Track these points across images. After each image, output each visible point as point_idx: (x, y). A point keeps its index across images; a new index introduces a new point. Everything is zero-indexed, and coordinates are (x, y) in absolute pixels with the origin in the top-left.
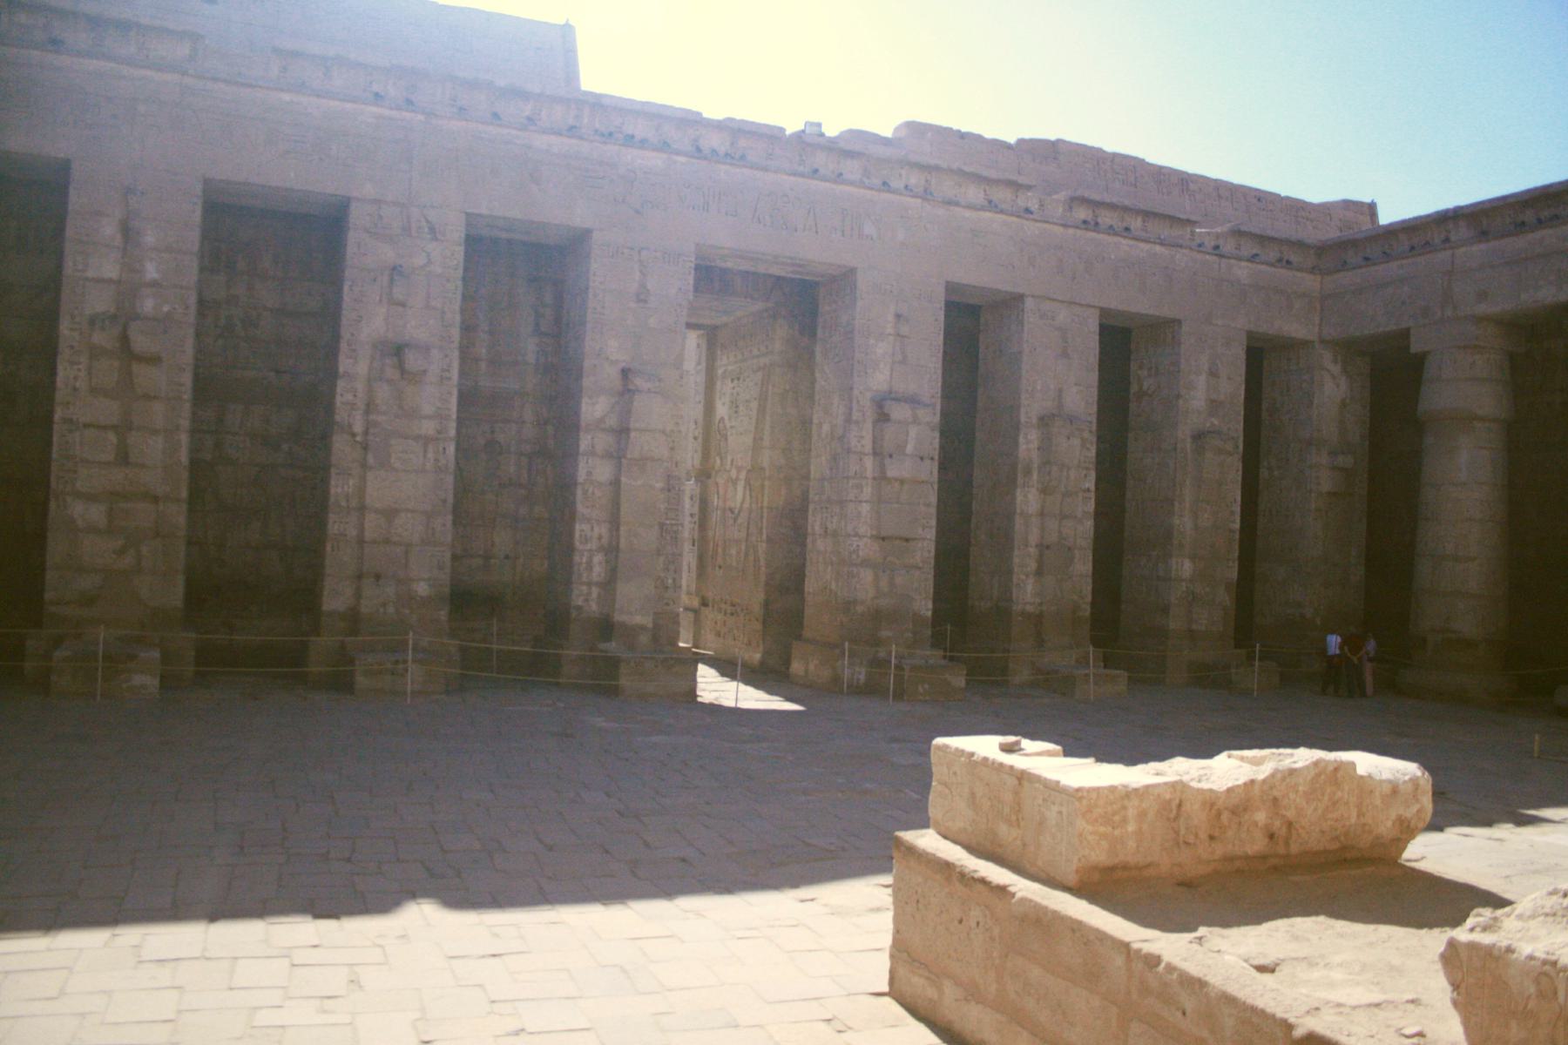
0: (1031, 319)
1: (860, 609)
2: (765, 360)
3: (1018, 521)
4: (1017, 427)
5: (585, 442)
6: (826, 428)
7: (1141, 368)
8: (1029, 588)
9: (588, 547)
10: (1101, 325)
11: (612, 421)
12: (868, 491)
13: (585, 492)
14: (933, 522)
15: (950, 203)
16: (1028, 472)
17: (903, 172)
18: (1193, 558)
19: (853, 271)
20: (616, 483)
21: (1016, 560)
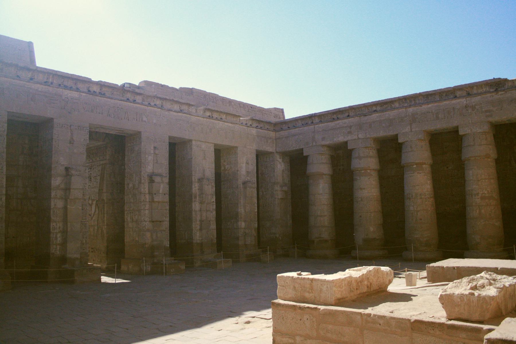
0: (194, 147)
1: (147, 246)
2: (104, 162)
3: (193, 213)
4: (191, 183)
5: (53, 194)
6: (131, 185)
7: (225, 162)
8: (198, 234)
9: (56, 231)
10: (215, 149)
11: (63, 186)
12: (147, 206)
13: (54, 212)
14: (168, 215)
15: (169, 110)
16: (195, 197)
17: (155, 100)
18: (245, 221)
19: (140, 133)
20: (65, 208)
21: (194, 226)
